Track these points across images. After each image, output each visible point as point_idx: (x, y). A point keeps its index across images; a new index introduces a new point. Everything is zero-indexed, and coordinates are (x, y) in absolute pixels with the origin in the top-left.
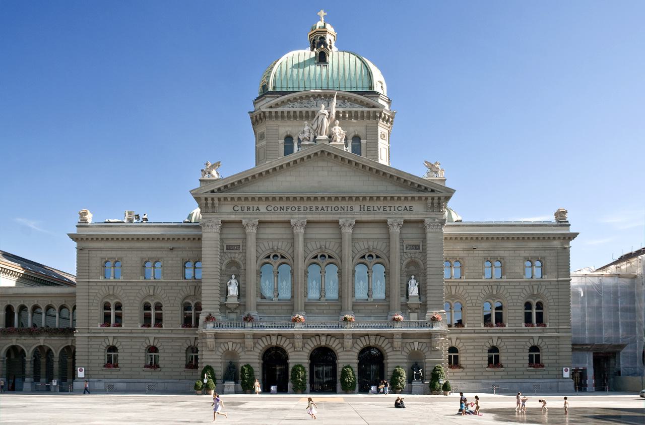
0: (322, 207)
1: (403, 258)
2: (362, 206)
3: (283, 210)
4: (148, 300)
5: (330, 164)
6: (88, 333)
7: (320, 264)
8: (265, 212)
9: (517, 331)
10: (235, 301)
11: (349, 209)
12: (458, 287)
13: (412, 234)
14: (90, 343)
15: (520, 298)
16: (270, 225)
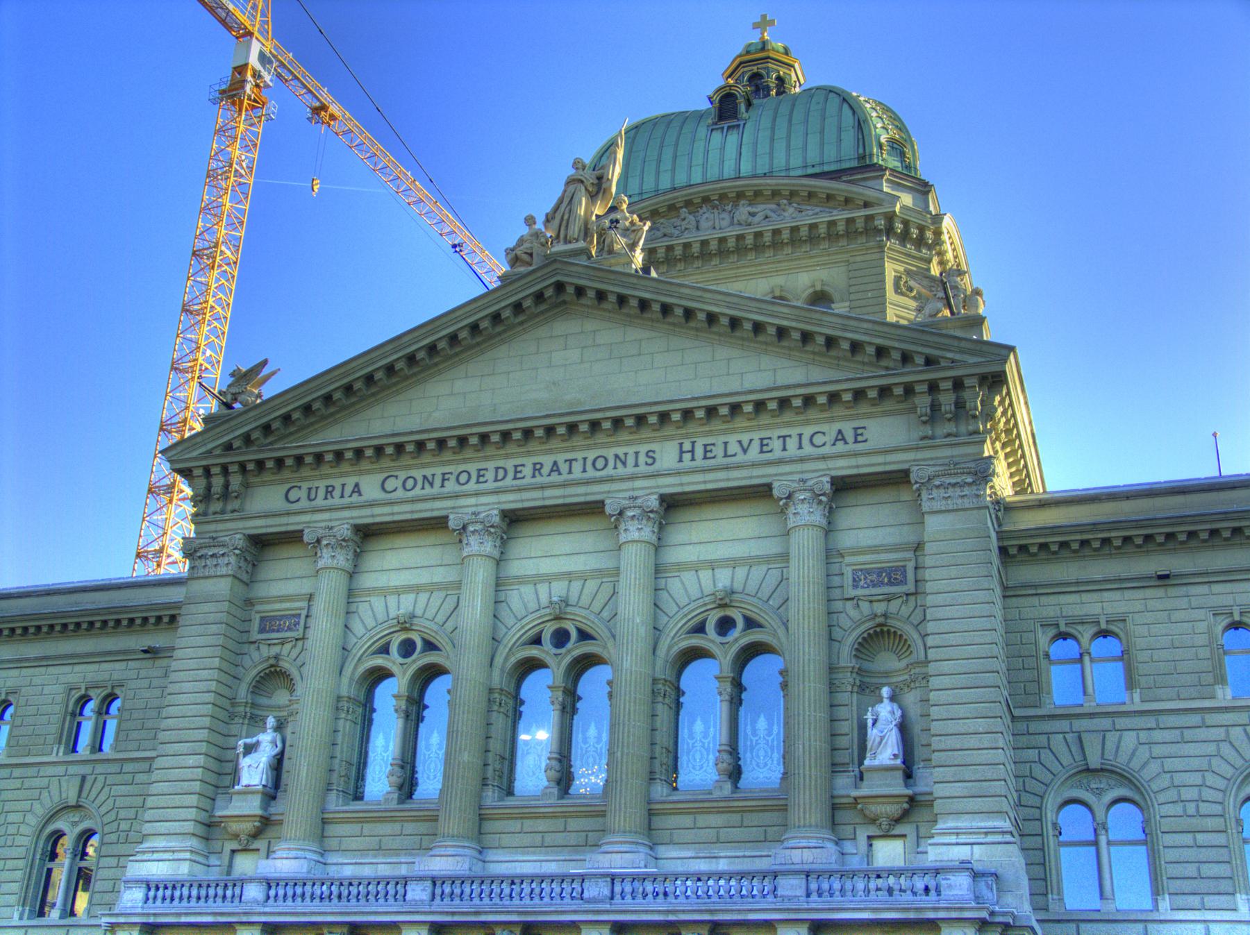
0: (555, 463)
1: (845, 622)
2: (687, 446)
4: (59, 824)
5: (590, 325)
7: (548, 660)
10: (253, 806)
11: (642, 459)
12: (1112, 738)
16: (400, 541)
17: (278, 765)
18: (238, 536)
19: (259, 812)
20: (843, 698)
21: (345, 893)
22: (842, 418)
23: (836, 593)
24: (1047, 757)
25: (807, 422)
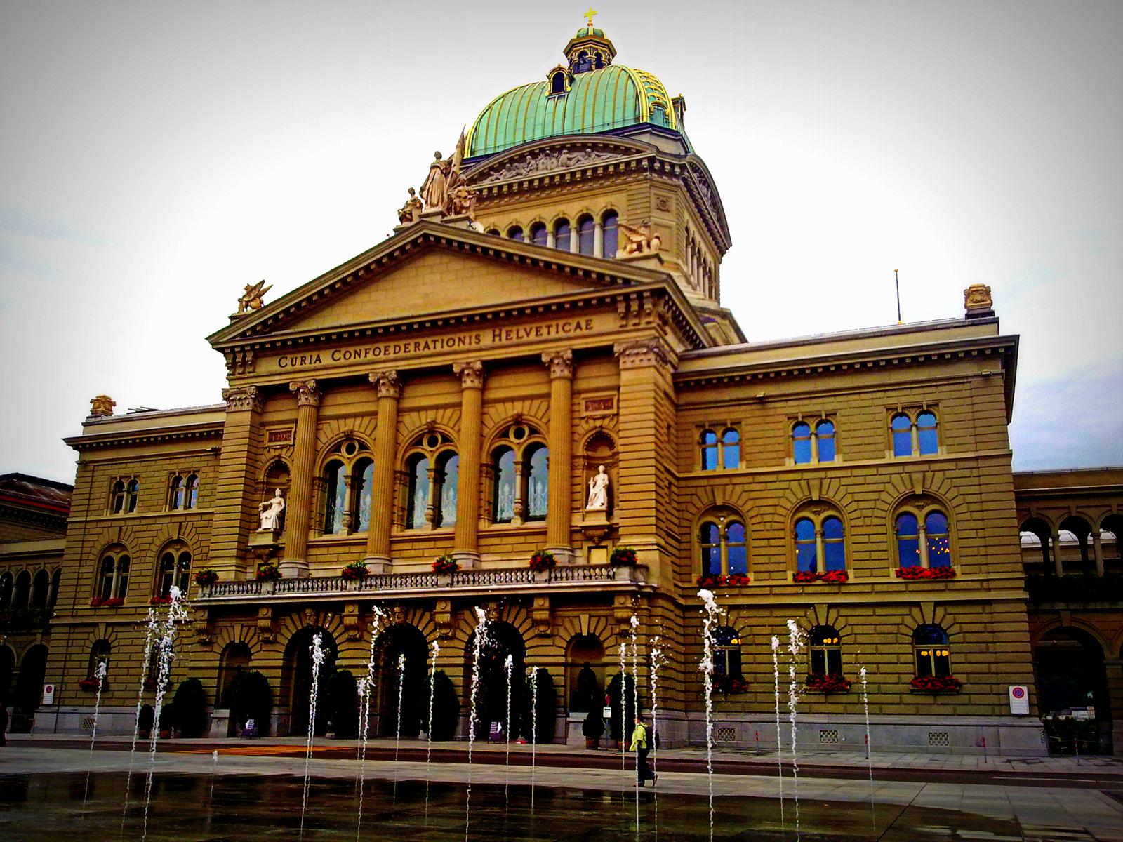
0: (427, 343)
2: (497, 332)
3: (360, 356)
5: (446, 259)
6: (72, 616)
8: (332, 364)
9: (878, 588)
12: (729, 488)
13: (595, 378)
14: (72, 636)
15: (879, 504)
17: (281, 517)
18: (253, 388)
19: (272, 543)
20: (578, 472)
21: (315, 586)
22: (580, 315)
23: (576, 415)
24: (695, 500)
25: (561, 318)
